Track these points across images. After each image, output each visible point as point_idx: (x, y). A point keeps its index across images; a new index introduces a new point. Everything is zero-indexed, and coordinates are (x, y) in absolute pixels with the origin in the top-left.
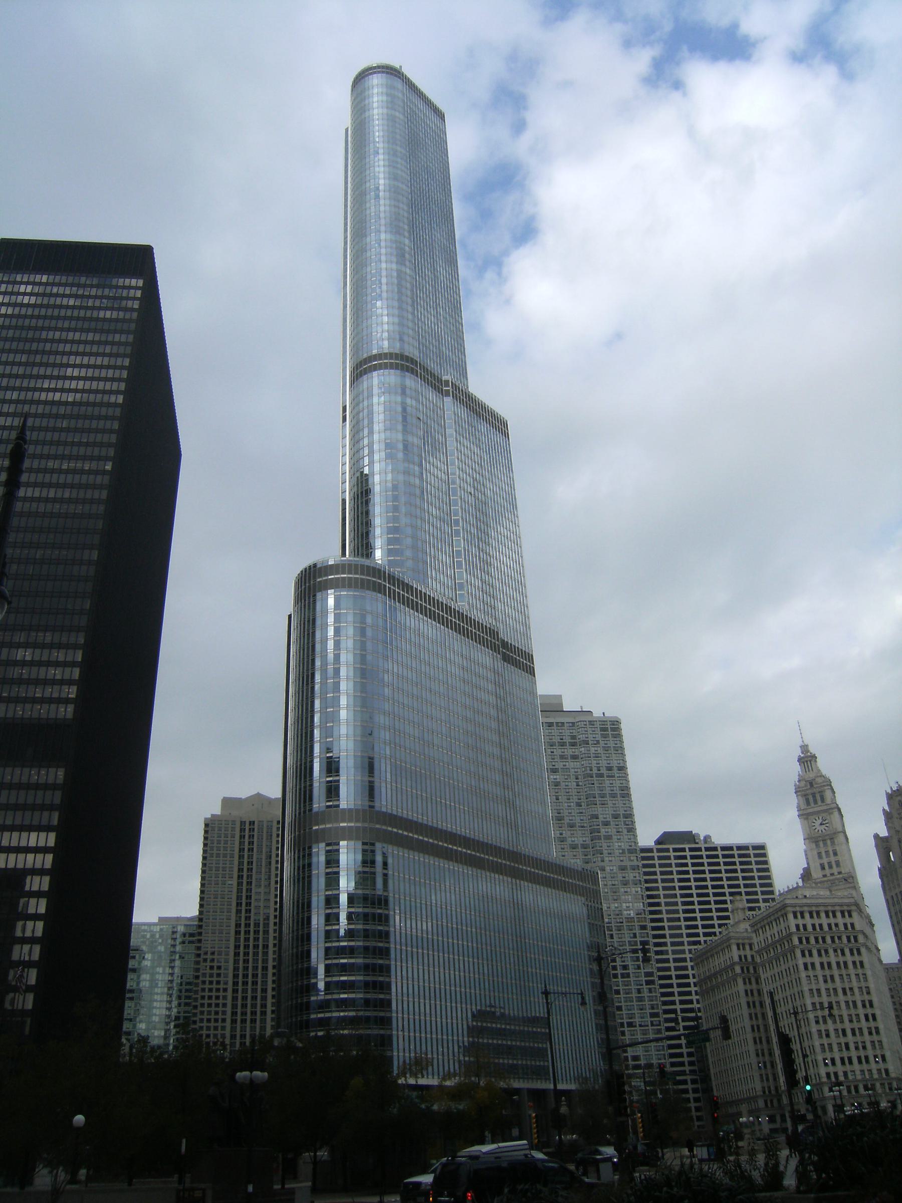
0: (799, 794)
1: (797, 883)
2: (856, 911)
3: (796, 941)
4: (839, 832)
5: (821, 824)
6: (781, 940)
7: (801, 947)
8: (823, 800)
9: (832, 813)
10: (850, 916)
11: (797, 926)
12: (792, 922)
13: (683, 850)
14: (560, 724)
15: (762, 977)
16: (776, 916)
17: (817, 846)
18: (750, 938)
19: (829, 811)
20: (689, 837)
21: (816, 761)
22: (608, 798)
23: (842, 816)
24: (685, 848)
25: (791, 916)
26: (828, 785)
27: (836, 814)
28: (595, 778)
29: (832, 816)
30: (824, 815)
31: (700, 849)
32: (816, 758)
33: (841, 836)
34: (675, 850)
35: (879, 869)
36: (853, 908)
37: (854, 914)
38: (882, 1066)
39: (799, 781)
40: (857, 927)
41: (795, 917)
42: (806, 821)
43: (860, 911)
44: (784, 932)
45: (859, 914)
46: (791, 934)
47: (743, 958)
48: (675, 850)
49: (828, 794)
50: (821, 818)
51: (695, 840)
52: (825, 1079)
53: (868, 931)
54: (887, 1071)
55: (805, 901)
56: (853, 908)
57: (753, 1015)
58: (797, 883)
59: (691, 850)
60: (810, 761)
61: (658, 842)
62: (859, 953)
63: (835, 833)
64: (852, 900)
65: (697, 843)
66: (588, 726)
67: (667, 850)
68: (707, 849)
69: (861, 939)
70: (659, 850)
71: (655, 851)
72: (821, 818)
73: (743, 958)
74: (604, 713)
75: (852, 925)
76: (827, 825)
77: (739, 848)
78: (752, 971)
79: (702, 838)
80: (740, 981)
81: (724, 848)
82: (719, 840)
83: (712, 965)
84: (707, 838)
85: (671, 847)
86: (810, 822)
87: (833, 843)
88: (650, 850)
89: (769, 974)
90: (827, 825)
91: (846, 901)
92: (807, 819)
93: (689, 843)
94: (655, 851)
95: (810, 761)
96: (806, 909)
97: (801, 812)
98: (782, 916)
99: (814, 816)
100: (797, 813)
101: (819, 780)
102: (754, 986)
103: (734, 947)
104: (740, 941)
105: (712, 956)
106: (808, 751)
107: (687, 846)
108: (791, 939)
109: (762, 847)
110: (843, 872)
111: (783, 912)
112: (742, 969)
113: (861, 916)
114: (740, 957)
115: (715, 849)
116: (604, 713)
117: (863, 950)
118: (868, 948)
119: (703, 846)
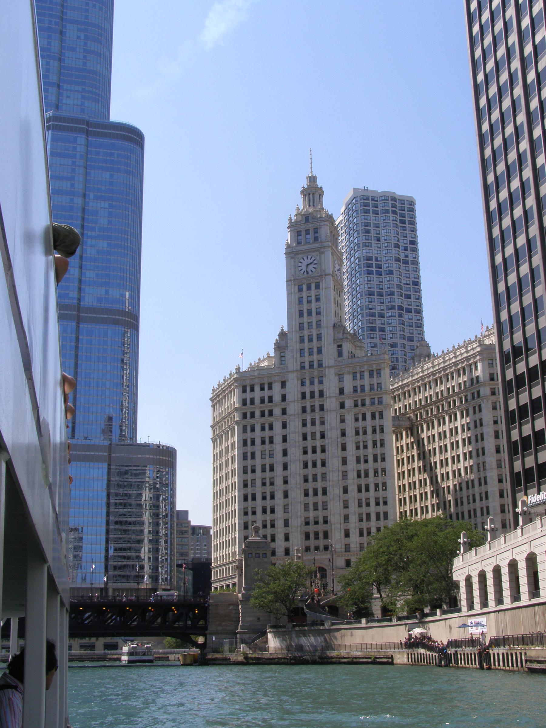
1: (268, 354)
4: (329, 275)
8: (316, 239)
9: (323, 253)
17: (300, 290)
29: (323, 256)
30: (314, 254)
42: (292, 260)
50: (309, 257)
58: (268, 354)
60: (313, 194)
72: (309, 257)
76: (315, 262)
87: (317, 286)
90: (315, 262)
92: (292, 258)
95: (313, 194)
99: (301, 256)
100: (284, 251)
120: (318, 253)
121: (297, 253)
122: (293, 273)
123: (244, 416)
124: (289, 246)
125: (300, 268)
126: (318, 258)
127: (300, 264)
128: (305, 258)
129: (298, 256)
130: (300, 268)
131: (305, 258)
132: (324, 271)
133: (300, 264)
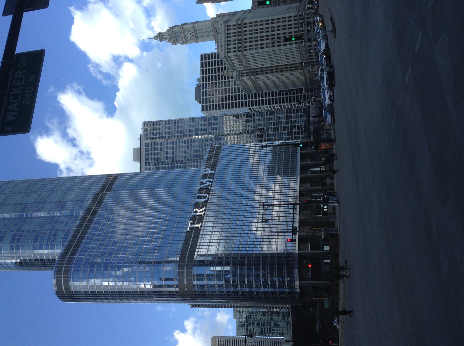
0: (176, 43)
2: (227, 23)
3: (240, 53)
5: (190, 34)
6: (239, 59)
7: (242, 51)
8: (179, 32)
9: (185, 29)
10: (230, 26)
11: (234, 52)
12: (232, 54)
13: (203, 92)
14: (146, 150)
15: (255, 67)
16: (229, 60)
18: (239, 71)
19: (184, 30)
20: (198, 89)
21: (162, 33)
22: (179, 129)
23: (186, 23)
24: (202, 91)
25: (229, 54)
26: (172, 29)
27: (185, 26)
28: (171, 135)
29: (186, 29)
30: (186, 32)
31: (203, 84)
32: (160, 33)
33: (195, 25)
34: (203, 96)
35: (212, 3)
36: (226, 24)
37: (229, 24)
38: (292, 19)
39: (170, 42)
40: (234, 23)
41: (230, 52)
42: (189, 41)
43: (228, 21)
44: (236, 58)
45: (229, 22)
46: (237, 55)
47: (247, 74)
48: (203, 96)
49: (176, 29)
51: (199, 86)
52: (297, 45)
53: (236, 17)
54: (295, 16)
55: (223, 47)
56: (226, 24)
57: (271, 71)
59: (203, 89)
61: (200, 102)
62: (245, 24)
63: (194, 28)
64: (223, 25)
65: (200, 85)
66: (147, 137)
67: (203, 99)
68: (203, 81)
69: (239, 22)
70: (203, 103)
71: (203, 105)
73: (247, 74)
74: (141, 129)
75: (234, 25)
77: (202, 66)
78: (253, 71)
79: (198, 83)
80: (257, 76)
81: (202, 74)
82: (199, 75)
83: (251, 87)
84: (198, 80)
85: (202, 97)
86: (189, 39)
88: (203, 107)
89: (254, 65)
91: (223, 27)
92: (188, 41)
93: (200, 90)
94: (203, 105)
96: (226, 47)
97: (185, 43)
98: (229, 58)
99: (187, 38)
100: (185, 45)
101: (170, 33)
102: (259, 70)
103: (243, 78)
104: (240, 75)
105: (247, 86)
106: (157, 36)
107: (202, 90)
108: (239, 55)
109: (202, 56)
110: (211, 26)
111: (228, 57)
112: (252, 75)
113: (230, 20)
114: (247, 75)
115: (203, 77)
116: (141, 129)
117: (245, 22)
118: (244, 19)
119: (201, 83)
120: (185, 31)
121: (185, 40)
122: (193, 40)
123: (240, 51)
124: (183, 44)
125: (191, 37)
126: (187, 30)
127: (190, 38)
128: (187, 36)
129: (187, 39)
130: (191, 37)
131: (187, 36)
132: (192, 27)
133: (190, 38)
